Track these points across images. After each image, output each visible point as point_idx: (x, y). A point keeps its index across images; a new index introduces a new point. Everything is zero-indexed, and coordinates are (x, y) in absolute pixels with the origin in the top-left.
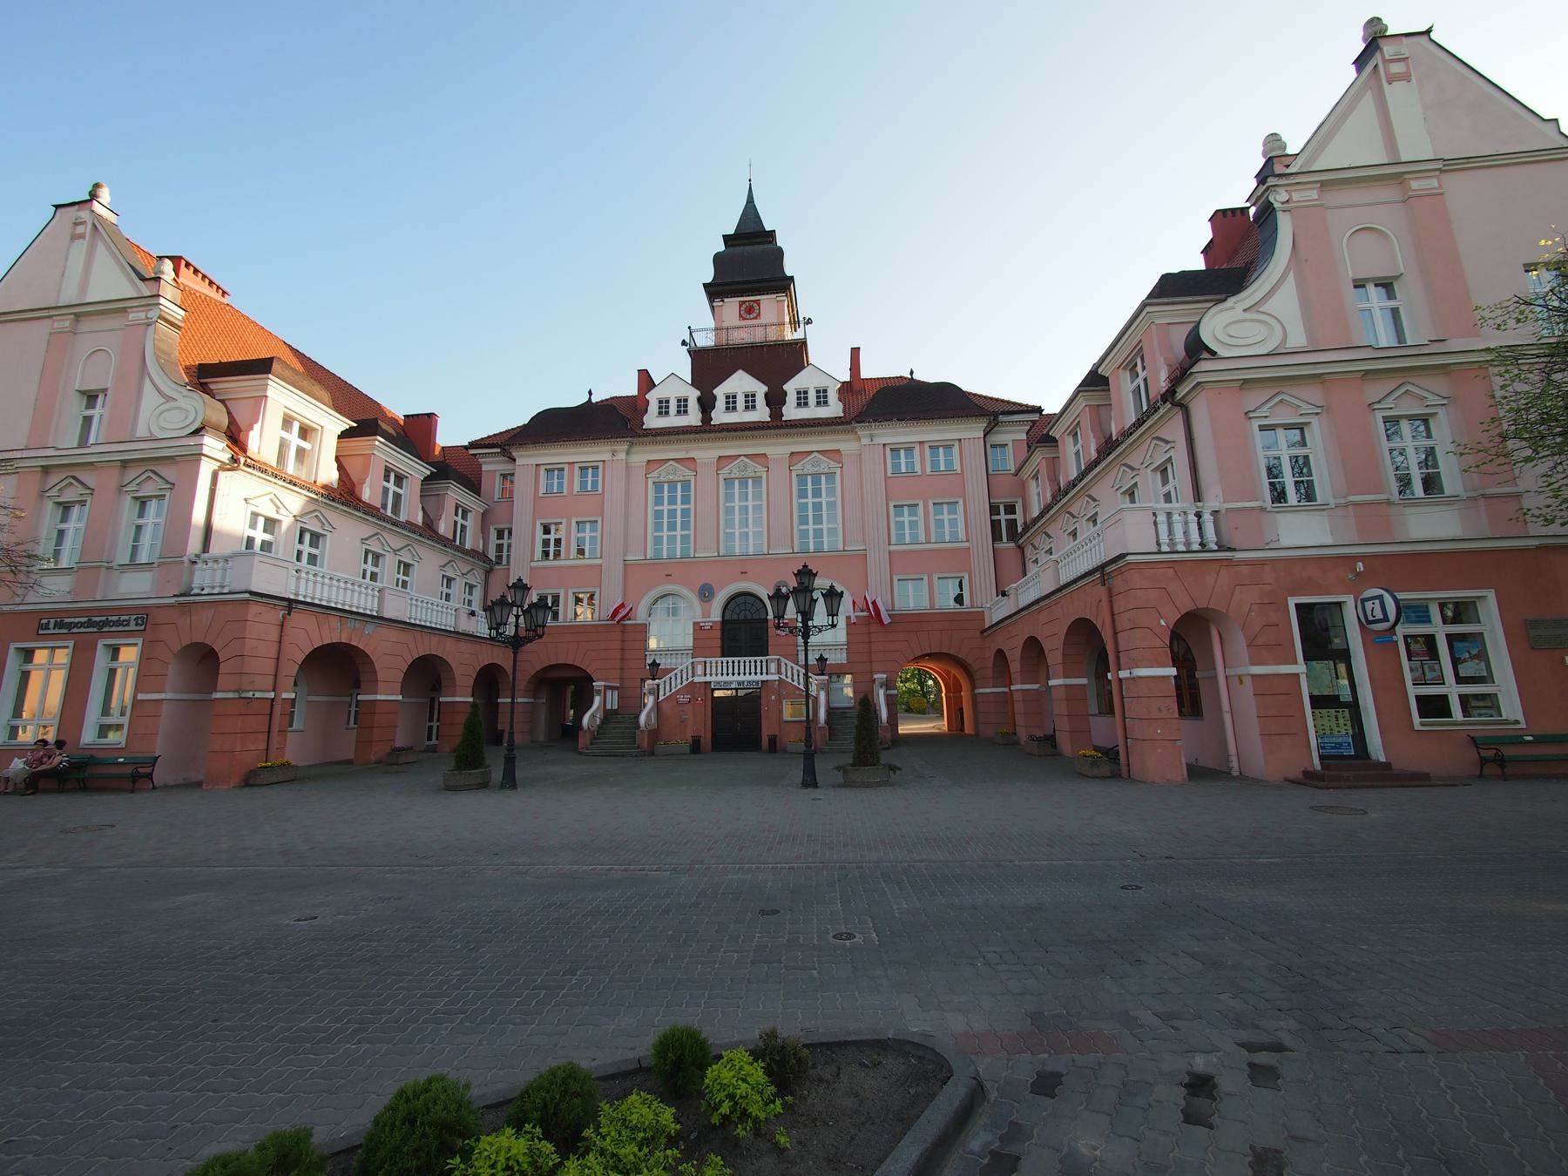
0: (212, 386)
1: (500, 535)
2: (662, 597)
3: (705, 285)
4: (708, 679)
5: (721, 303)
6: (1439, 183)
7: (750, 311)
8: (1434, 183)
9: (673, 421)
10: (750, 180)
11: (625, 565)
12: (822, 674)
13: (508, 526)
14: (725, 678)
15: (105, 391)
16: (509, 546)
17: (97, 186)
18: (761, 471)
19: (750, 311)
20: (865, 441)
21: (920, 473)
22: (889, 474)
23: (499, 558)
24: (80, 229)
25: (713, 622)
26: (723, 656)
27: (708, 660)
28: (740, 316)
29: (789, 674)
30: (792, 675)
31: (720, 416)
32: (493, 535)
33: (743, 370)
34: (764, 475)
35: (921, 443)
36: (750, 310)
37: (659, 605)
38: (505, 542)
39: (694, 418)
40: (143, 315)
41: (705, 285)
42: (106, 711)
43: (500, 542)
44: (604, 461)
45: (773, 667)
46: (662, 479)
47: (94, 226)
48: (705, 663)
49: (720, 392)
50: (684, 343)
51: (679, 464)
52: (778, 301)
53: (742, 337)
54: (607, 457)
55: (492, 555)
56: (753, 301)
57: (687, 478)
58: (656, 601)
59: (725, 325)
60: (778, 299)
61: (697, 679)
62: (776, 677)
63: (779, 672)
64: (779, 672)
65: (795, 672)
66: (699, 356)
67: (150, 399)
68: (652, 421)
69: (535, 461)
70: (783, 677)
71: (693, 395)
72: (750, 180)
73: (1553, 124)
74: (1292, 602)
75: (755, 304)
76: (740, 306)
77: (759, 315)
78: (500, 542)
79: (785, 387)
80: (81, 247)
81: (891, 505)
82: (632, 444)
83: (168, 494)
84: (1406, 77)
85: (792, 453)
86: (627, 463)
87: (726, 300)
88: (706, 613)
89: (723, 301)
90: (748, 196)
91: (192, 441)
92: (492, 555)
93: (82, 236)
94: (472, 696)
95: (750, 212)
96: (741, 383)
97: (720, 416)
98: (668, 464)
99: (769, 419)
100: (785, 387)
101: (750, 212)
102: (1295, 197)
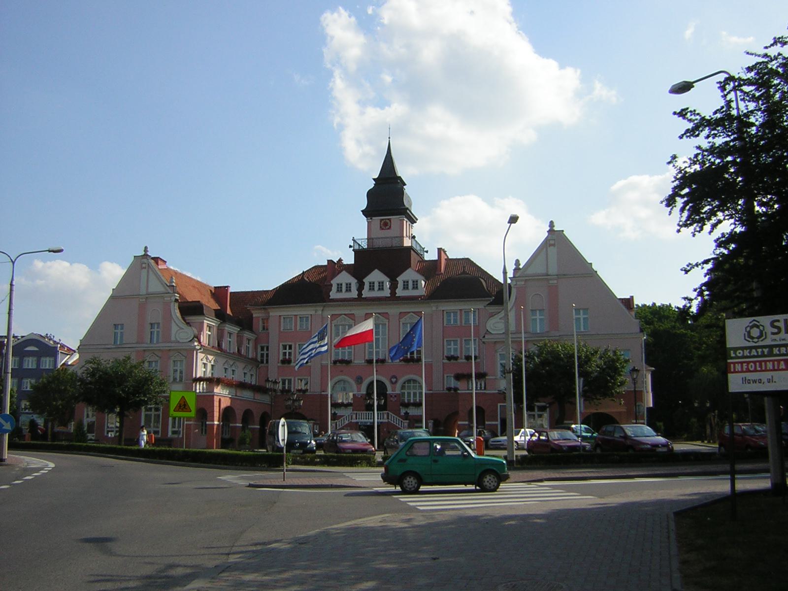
0: (186, 318)
1: (262, 349)
2: (338, 381)
3: (362, 211)
4: (358, 420)
5: (370, 220)
6: (557, 281)
7: (385, 225)
8: (555, 282)
9: (344, 295)
10: (389, 138)
11: (322, 366)
12: (406, 420)
13: (267, 345)
14: (365, 420)
15: (158, 324)
16: (267, 355)
17: (146, 248)
18: (386, 321)
19: (385, 225)
20: (434, 308)
21: (459, 325)
22: (445, 325)
23: (262, 362)
24: (144, 265)
25: (362, 394)
26: (366, 411)
27: (358, 412)
28: (381, 227)
29: (392, 420)
30: (394, 419)
31: (366, 293)
32: (259, 349)
33: (379, 270)
34: (387, 323)
35: (461, 310)
36: (386, 224)
37: (337, 385)
38: (265, 352)
39: (354, 294)
40: (169, 299)
41: (362, 211)
42: (173, 427)
43: (262, 352)
44: (311, 315)
45: (385, 416)
46: (339, 324)
47: (148, 264)
48: (357, 414)
49: (366, 280)
50: (350, 247)
51: (347, 316)
52: (401, 220)
53: (380, 244)
54: (313, 313)
55: (259, 359)
56: (388, 219)
57: (351, 323)
58: (336, 383)
59: (373, 237)
60: (401, 219)
61: (353, 421)
62: (387, 421)
63: (388, 418)
64: (388, 418)
65: (395, 418)
66: (359, 254)
67: (174, 328)
68: (334, 294)
69: (279, 314)
70: (390, 421)
71: (354, 282)
72: (389, 138)
73: (590, 265)
74: (499, 405)
75: (388, 221)
76: (381, 222)
77: (390, 227)
78: (262, 352)
79: (397, 279)
80: (144, 272)
81: (445, 340)
82: (324, 306)
83: (184, 360)
84: (553, 245)
85: (401, 313)
86: (322, 315)
87: (373, 218)
88: (359, 390)
89: (371, 219)
90: (387, 152)
91: (189, 344)
92: (259, 359)
93: (145, 268)
94: (242, 423)
95: (389, 163)
96: (376, 276)
97: (366, 293)
98: (341, 317)
99: (389, 295)
100: (397, 279)
101: (389, 163)
102: (518, 283)
